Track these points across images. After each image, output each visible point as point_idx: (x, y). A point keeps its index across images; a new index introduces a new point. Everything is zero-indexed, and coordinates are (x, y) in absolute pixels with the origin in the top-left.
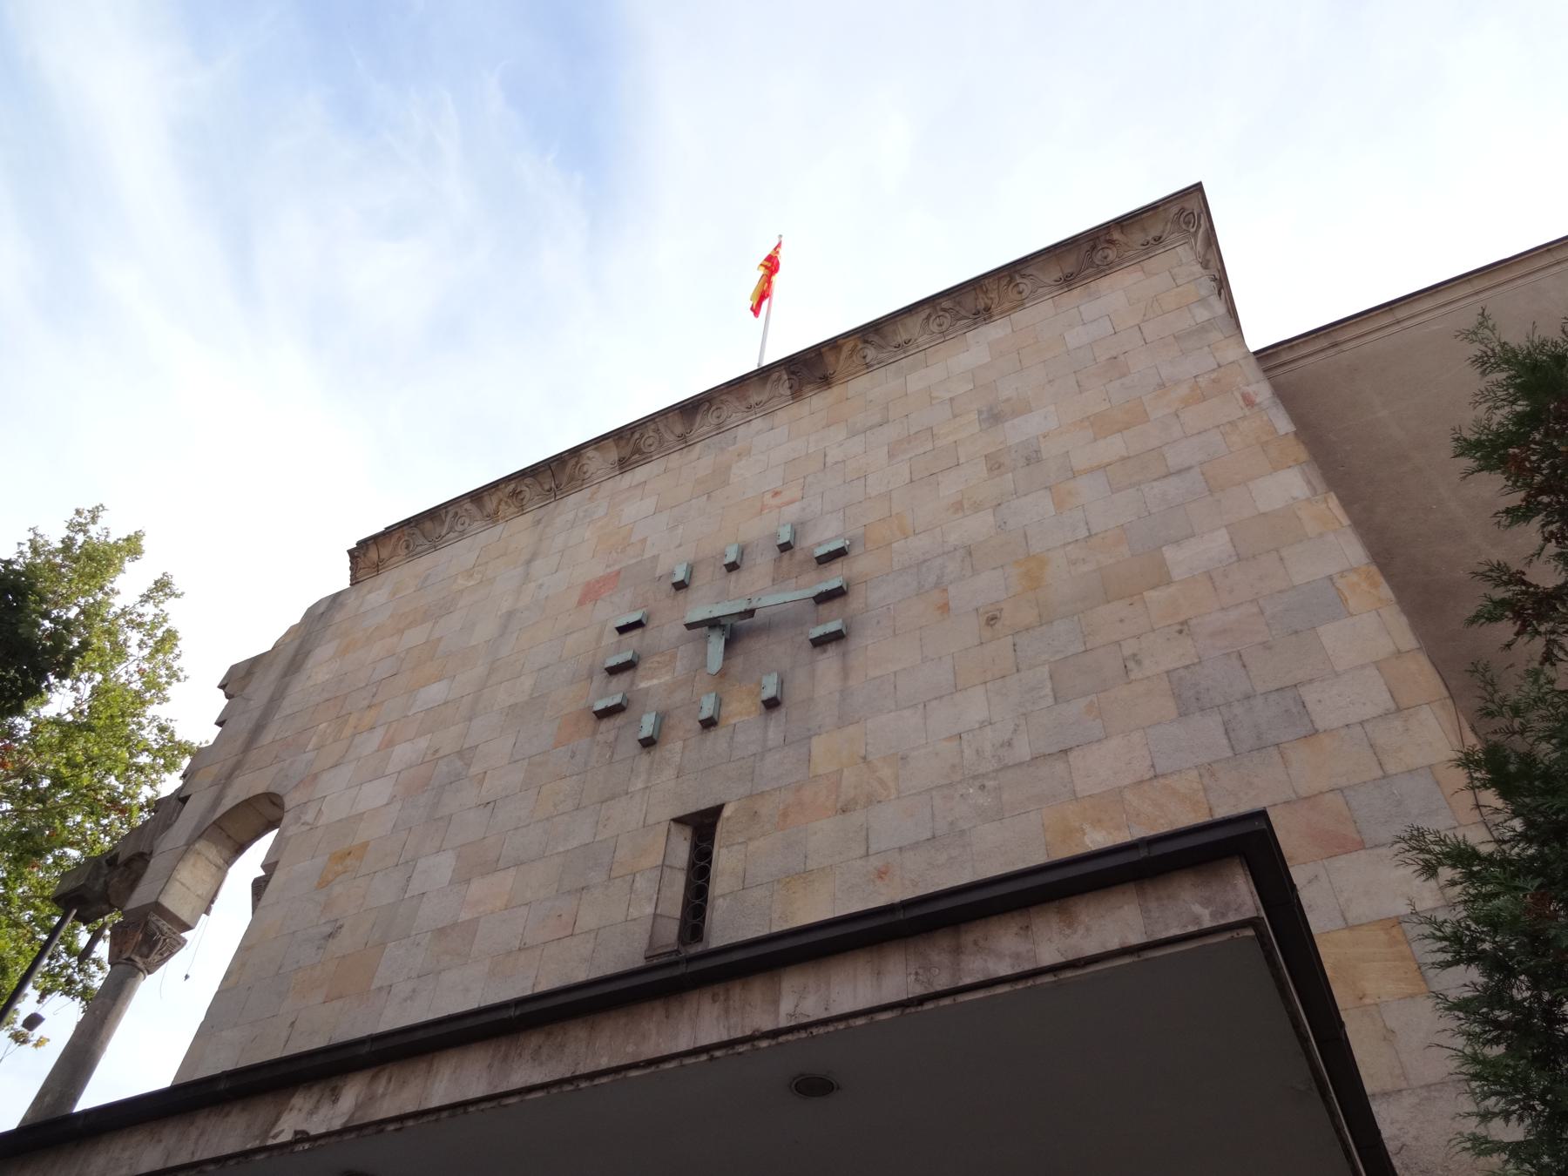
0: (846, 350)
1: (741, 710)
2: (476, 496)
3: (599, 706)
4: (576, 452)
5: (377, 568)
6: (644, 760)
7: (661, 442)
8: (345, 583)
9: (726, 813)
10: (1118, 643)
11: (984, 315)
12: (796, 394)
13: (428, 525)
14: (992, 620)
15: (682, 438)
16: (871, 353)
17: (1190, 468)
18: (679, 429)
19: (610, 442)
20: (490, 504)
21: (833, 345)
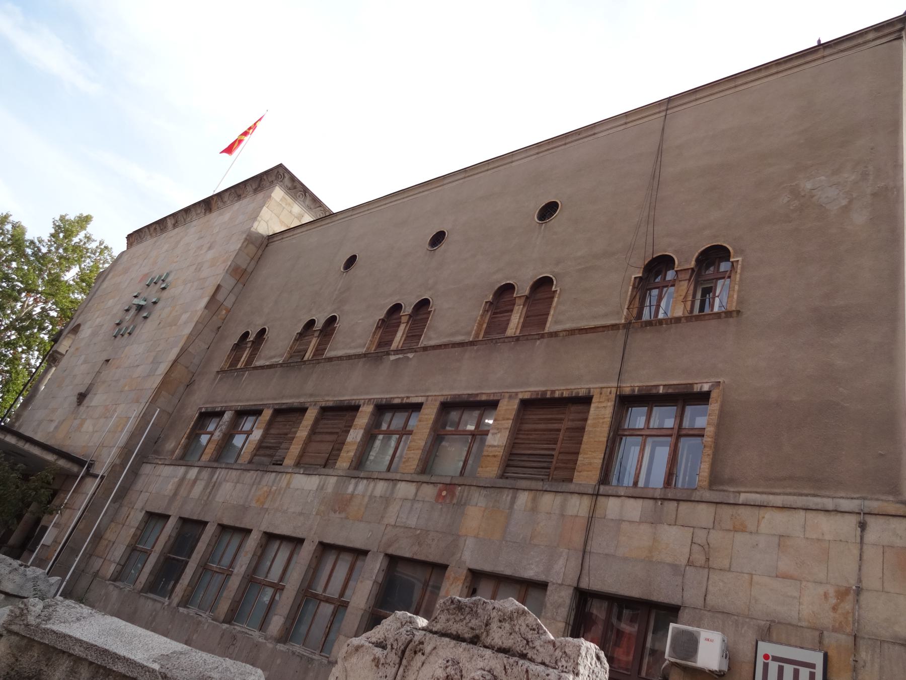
2: (148, 227)
4: (165, 218)
8: (124, 248)
19: (171, 217)
20: (152, 229)
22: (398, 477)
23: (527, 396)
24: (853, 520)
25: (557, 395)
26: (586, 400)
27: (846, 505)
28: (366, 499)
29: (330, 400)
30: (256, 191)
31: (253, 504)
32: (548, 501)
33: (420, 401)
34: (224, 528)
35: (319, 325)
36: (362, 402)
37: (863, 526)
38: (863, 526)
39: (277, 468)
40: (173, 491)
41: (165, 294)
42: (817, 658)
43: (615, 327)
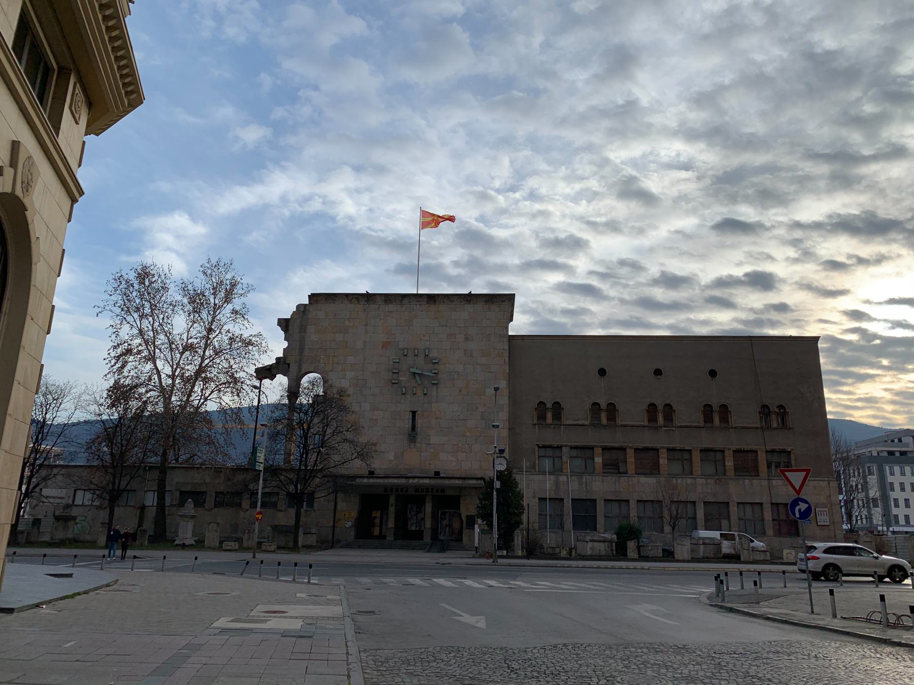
0: (440, 297)
1: (419, 392)
2: (347, 295)
3: (393, 382)
5: (317, 302)
6: (403, 396)
7: (395, 301)
9: (419, 412)
10: (476, 404)
11: (469, 302)
12: (428, 303)
13: (332, 296)
14: (460, 391)
15: (401, 301)
16: (445, 300)
17: (492, 372)
18: (400, 299)
20: (350, 298)
21: (438, 295)
22: (696, 477)
23: (735, 449)
24: (827, 482)
25: (746, 449)
26: (756, 452)
27: (827, 479)
28: (685, 485)
29: (641, 445)
30: (486, 302)
31: (622, 490)
32: (756, 482)
33: (690, 448)
34: (606, 501)
35: (603, 406)
36: (659, 448)
37: (829, 483)
38: (829, 483)
39: (627, 475)
40: (554, 488)
41: (441, 367)
42: (827, 510)
43: (757, 428)
